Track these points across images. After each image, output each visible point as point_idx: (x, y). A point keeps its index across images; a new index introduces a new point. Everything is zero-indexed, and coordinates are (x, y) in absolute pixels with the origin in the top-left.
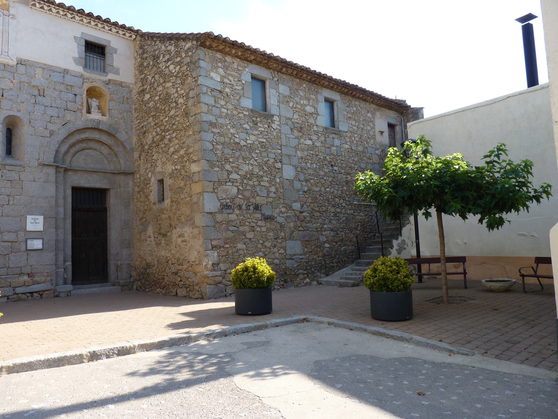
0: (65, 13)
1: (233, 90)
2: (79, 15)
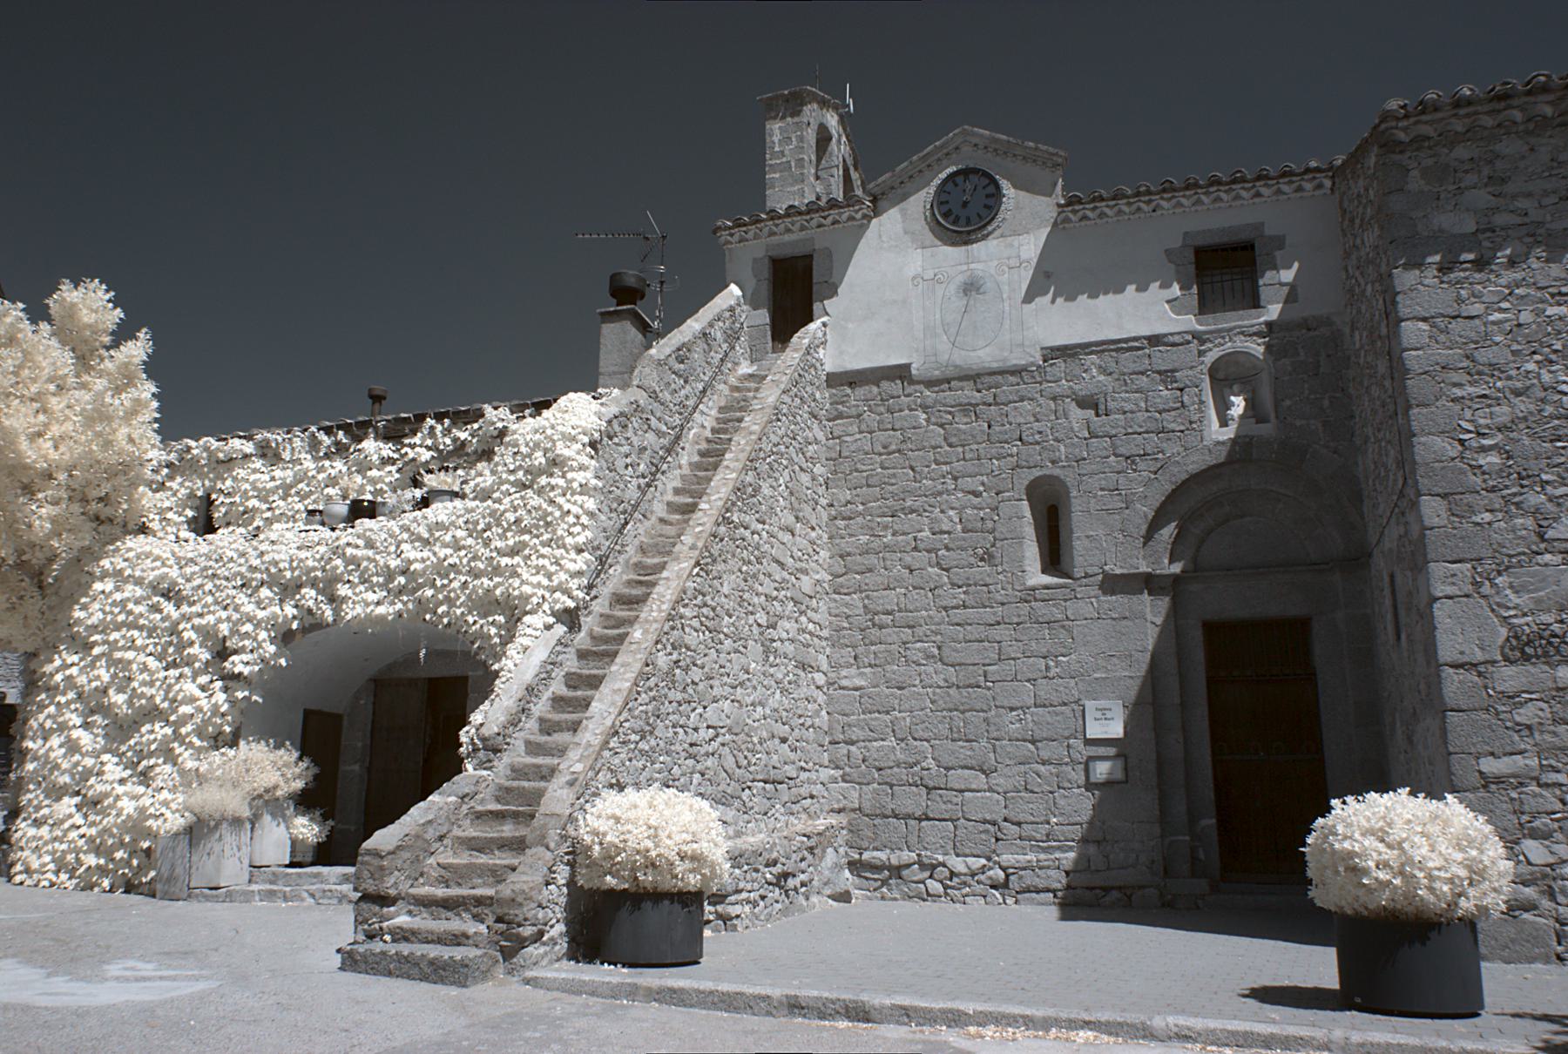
0: (1134, 207)
1: (1540, 239)
2: (1165, 196)
